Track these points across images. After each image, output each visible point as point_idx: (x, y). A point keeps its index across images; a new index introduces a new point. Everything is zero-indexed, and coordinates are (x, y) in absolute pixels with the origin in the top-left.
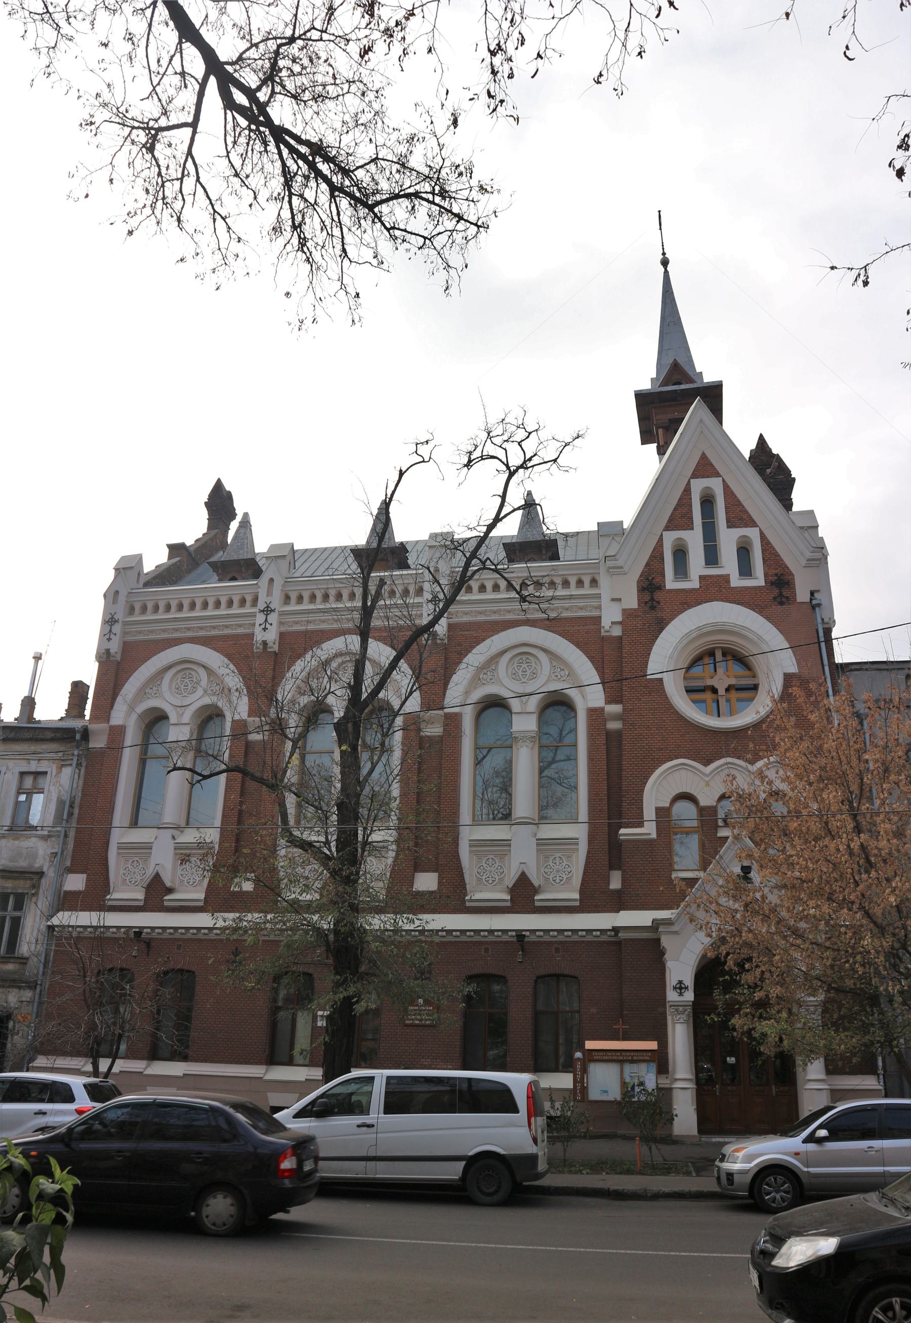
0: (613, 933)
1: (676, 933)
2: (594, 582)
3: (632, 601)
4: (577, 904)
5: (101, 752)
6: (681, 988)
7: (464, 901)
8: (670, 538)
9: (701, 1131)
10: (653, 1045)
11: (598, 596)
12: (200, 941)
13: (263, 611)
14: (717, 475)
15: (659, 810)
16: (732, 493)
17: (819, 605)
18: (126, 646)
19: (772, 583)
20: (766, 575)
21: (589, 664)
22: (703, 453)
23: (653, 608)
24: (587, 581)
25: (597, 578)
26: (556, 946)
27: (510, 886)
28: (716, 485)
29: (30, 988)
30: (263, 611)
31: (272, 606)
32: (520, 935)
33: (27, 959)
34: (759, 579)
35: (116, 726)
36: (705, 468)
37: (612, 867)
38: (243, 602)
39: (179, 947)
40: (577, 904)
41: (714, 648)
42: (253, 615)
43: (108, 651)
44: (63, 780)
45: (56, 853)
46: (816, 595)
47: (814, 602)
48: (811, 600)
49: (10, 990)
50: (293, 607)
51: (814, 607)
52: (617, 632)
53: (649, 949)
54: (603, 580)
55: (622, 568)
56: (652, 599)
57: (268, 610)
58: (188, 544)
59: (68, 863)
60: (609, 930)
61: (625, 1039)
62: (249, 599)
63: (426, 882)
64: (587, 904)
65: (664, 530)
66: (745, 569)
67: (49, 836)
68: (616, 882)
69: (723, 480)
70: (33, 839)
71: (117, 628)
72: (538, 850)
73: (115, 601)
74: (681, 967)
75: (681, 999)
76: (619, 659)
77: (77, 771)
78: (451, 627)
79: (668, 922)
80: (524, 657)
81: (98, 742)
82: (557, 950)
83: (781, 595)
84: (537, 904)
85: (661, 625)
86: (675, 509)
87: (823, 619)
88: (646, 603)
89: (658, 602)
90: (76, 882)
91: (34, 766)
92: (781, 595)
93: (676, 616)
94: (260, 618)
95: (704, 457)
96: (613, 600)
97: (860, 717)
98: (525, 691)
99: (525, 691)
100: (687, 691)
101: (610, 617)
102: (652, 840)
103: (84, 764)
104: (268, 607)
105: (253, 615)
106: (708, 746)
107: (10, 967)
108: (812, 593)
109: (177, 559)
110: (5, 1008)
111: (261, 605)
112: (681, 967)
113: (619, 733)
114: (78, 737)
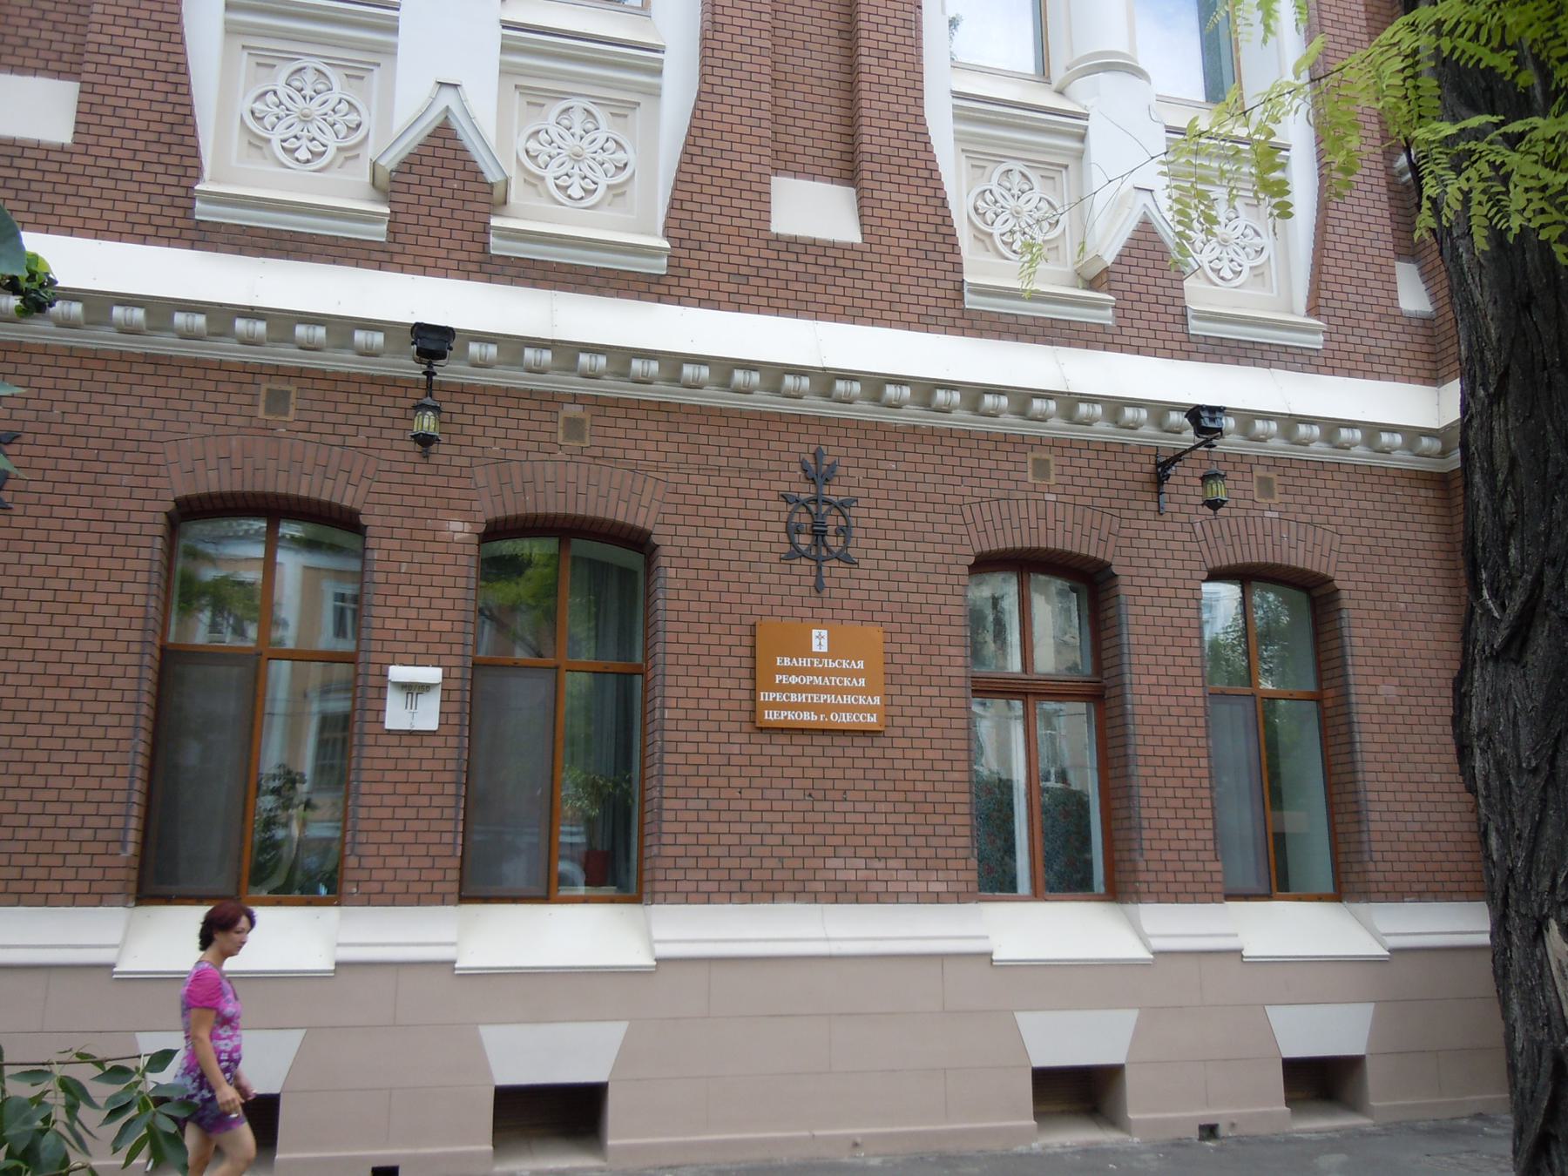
63: (812, 210)
82: (1266, 484)
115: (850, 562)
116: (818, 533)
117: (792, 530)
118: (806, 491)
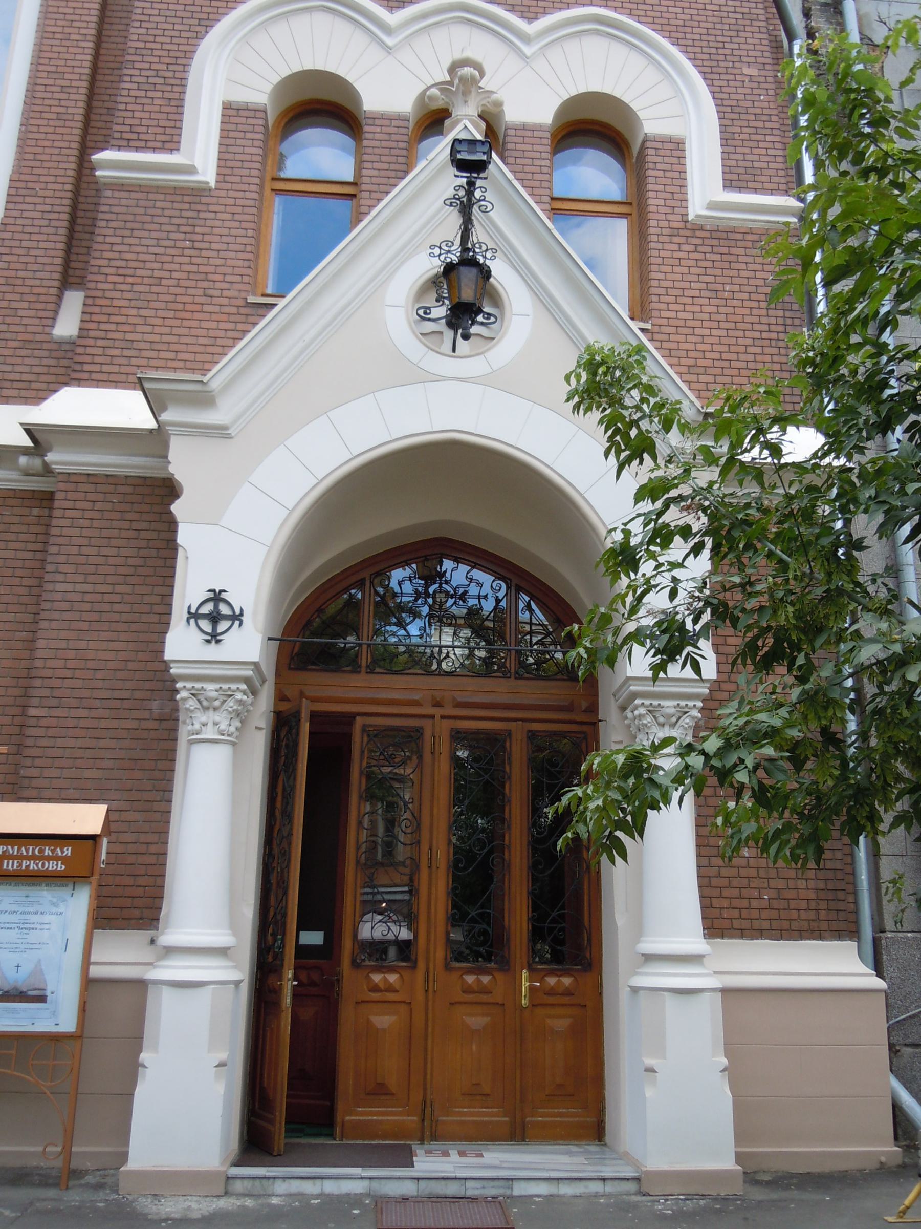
1: (220, 432)
9: (257, 1140)
15: (234, 115)
74: (235, 551)
75: (213, 652)
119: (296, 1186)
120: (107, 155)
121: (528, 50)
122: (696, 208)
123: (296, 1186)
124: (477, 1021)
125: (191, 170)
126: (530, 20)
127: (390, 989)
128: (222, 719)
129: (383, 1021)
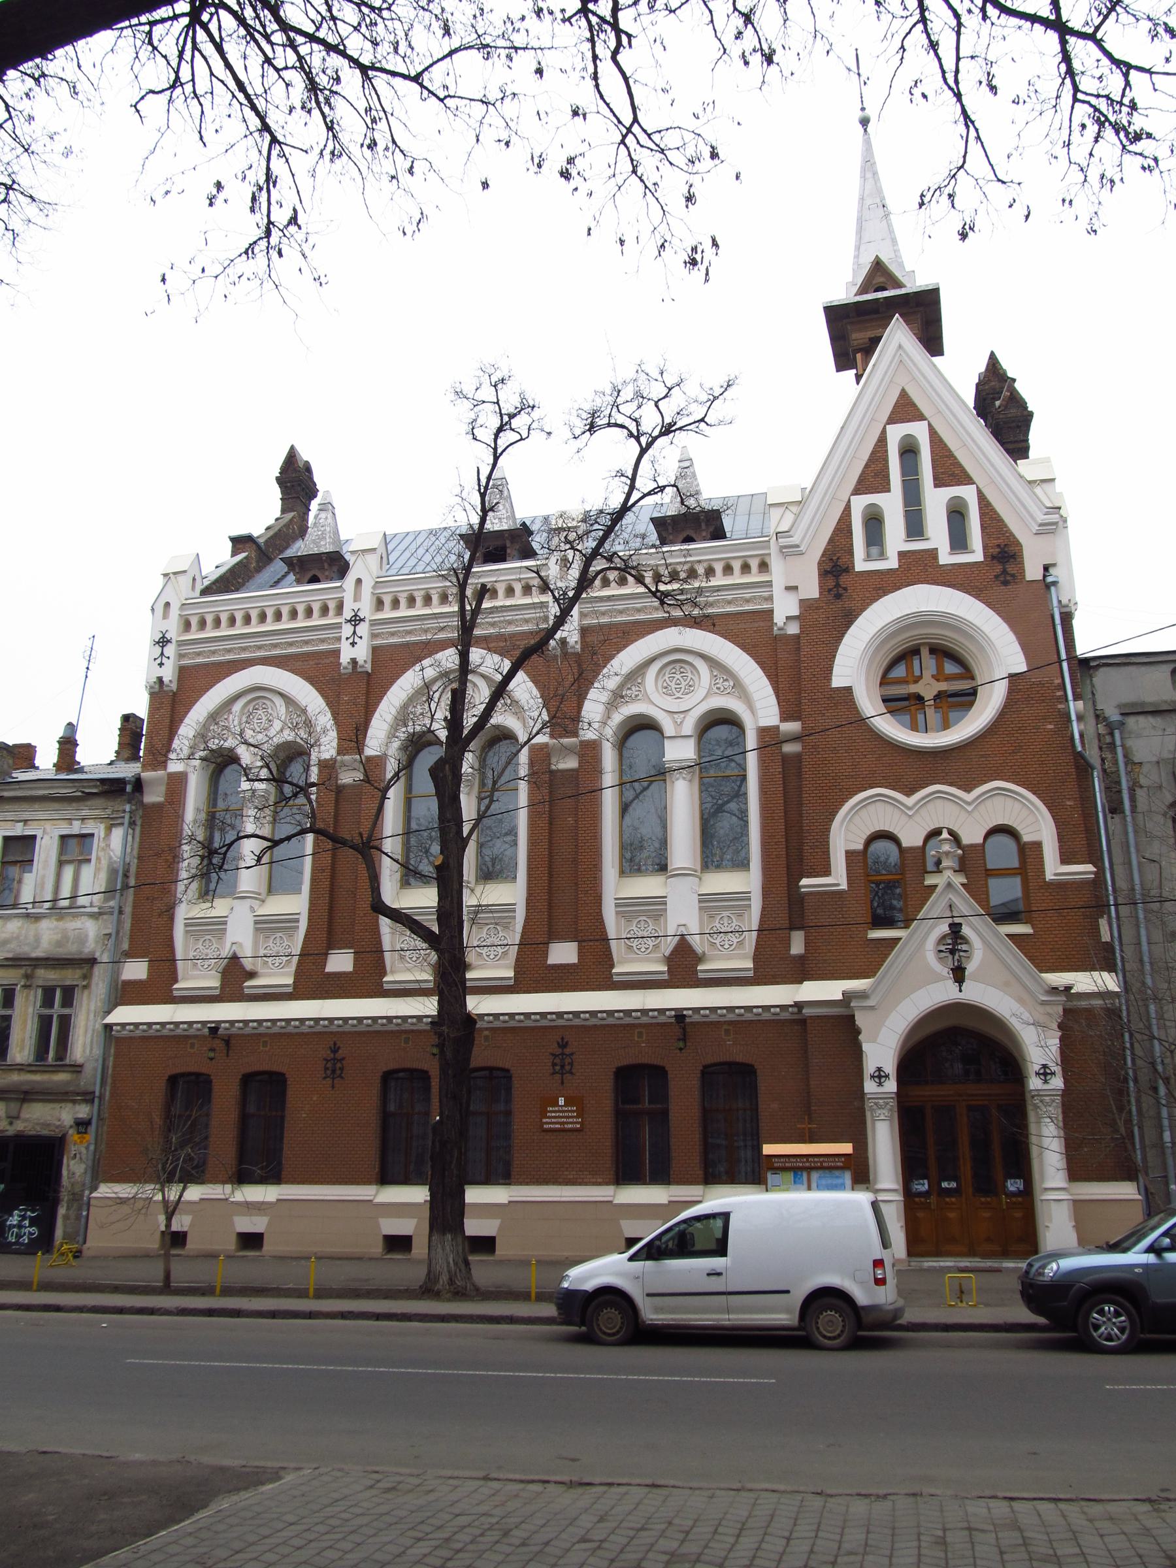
0: (795, 1010)
1: (872, 1008)
2: (764, 566)
3: (811, 589)
4: (751, 974)
5: (158, 807)
6: (880, 1077)
7: (611, 975)
8: (860, 503)
10: (846, 1148)
11: (769, 584)
12: (290, 1035)
13: (350, 621)
14: (921, 417)
15: (849, 854)
16: (941, 440)
17: (1055, 583)
18: (183, 672)
19: (993, 557)
20: (985, 547)
21: (759, 672)
22: (903, 390)
23: (838, 596)
24: (754, 564)
25: (767, 560)
26: (725, 1027)
27: (667, 954)
28: (919, 430)
29: (86, 1101)
30: (350, 621)
31: (361, 615)
32: (680, 1016)
33: (81, 1066)
34: (976, 554)
35: (175, 773)
36: (905, 410)
37: (793, 928)
38: (325, 610)
39: (265, 1044)
40: (751, 974)
41: (920, 645)
42: (338, 626)
43: (160, 680)
44: (114, 844)
45: (110, 935)
46: (1052, 571)
47: (1049, 579)
48: (1045, 576)
49: (63, 1105)
50: (388, 614)
51: (1048, 586)
52: (793, 629)
53: (841, 1027)
54: (776, 564)
55: (798, 546)
56: (837, 585)
57: (356, 620)
58: (255, 535)
59: (126, 946)
60: (791, 1006)
61: (812, 1140)
62: (332, 605)
63: (564, 953)
64: (762, 975)
65: (853, 494)
66: (959, 541)
67: (100, 914)
68: (797, 945)
69: (930, 425)
70: (84, 918)
71: (170, 650)
72: (701, 908)
73: (165, 616)
74: (881, 1050)
75: (880, 1090)
76: (797, 662)
77: (130, 831)
78: (584, 631)
79: (862, 995)
80: (678, 666)
81: (153, 796)
82: (727, 1031)
83: (1004, 572)
84: (701, 975)
85: (848, 618)
86: (867, 466)
87: (1060, 602)
88: (830, 590)
89: (845, 589)
90: (136, 970)
91: (76, 828)
92: (1004, 572)
93: (869, 605)
94: (347, 630)
95: (904, 394)
96: (788, 588)
97: (1111, 728)
98: (678, 709)
99: (678, 709)
100: (884, 701)
101: (785, 609)
102: (841, 892)
103: (139, 822)
104: (356, 615)
105: (338, 626)
106: (914, 770)
107: (62, 1077)
108: (1046, 568)
109: (244, 555)
110: (57, 1127)
111: (348, 614)
112: (881, 1050)
113: (798, 757)
114: (129, 788)
115: (572, 1073)
116: (562, 1065)
117: (554, 1065)
118: (559, 1051)
119: (931, 1264)
120: (804, 881)
121: (970, 808)
122: (1049, 876)
123: (931, 1264)
124: (987, 1215)
125: (838, 885)
126: (968, 790)
127: (953, 1203)
128: (886, 1112)
129: (952, 1215)
